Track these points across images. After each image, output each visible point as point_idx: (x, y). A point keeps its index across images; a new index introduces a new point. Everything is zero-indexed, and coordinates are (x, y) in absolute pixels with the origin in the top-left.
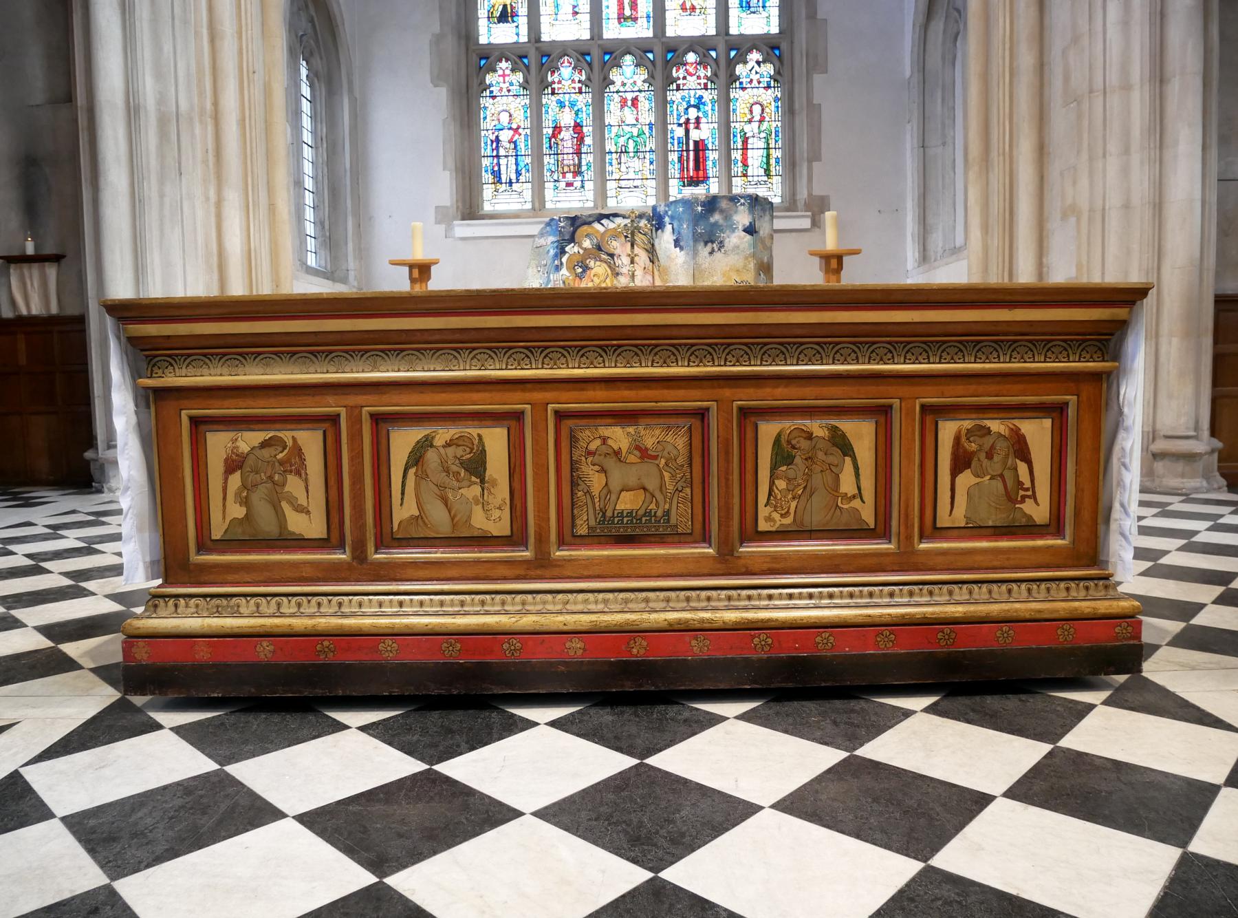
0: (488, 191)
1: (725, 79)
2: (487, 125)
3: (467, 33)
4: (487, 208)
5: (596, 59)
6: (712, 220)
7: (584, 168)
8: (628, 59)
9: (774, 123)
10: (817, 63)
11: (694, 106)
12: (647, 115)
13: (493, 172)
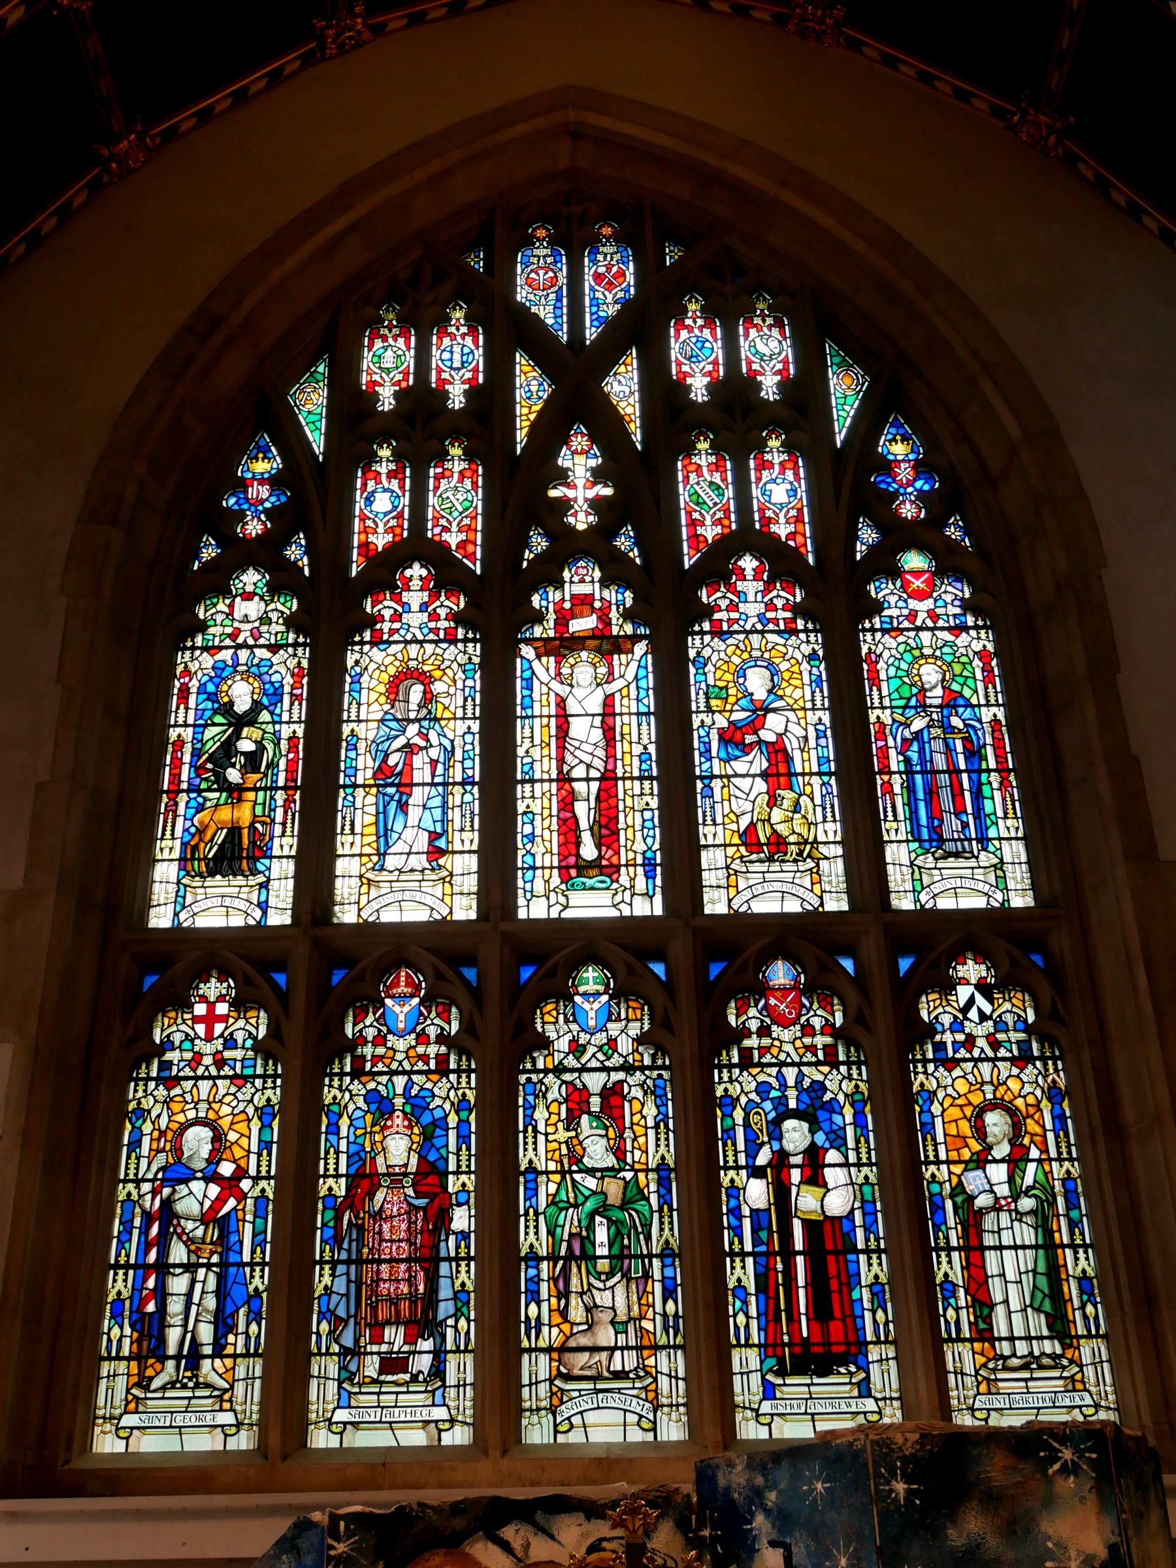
0: (113, 1385)
4: (107, 1444)
5: (497, 977)
6: (956, 1537)
7: (445, 1309)
8: (591, 978)
9: (1056, 1165)
11: (797, 1114)
13: (140, 1321)
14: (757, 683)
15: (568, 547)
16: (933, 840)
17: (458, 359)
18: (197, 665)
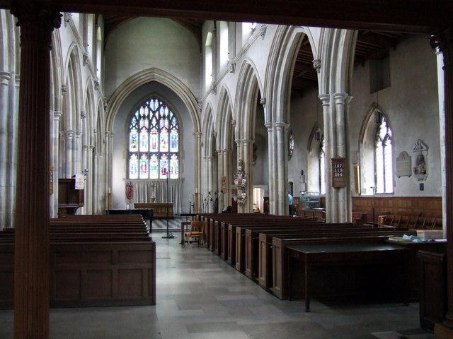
1: (169, 158)
2: (131, 165)
3: (128, 149)
5: (149, 155)
9: (177, 165)
10: (183, 158)
15: (153, 127)
16: (173, 147)
17: (147, 109)
18: (131, 134)
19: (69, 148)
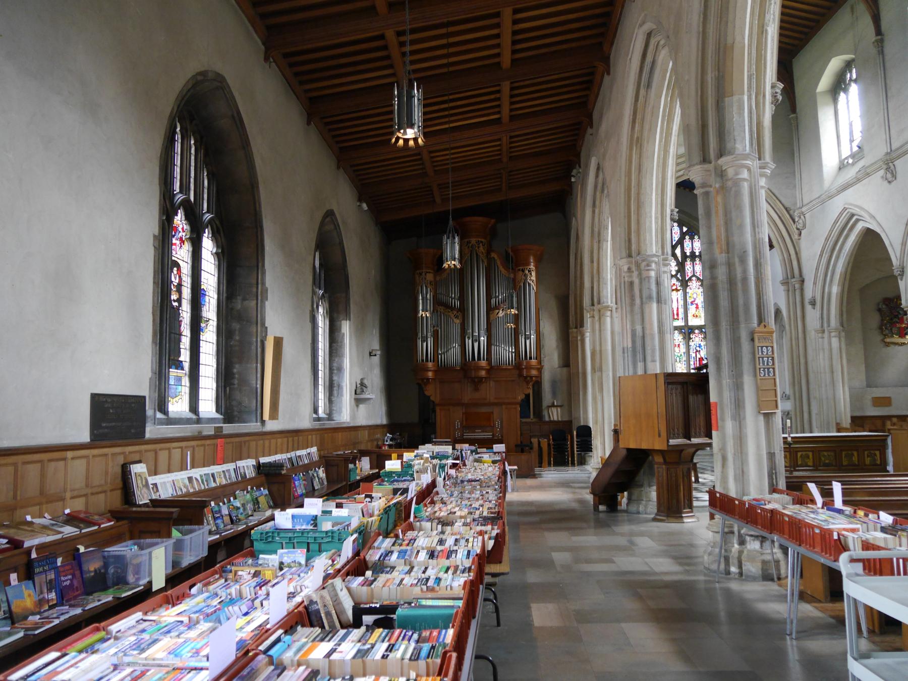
12: (683, 349)
14: (695, 296)
19: (650, 298)
